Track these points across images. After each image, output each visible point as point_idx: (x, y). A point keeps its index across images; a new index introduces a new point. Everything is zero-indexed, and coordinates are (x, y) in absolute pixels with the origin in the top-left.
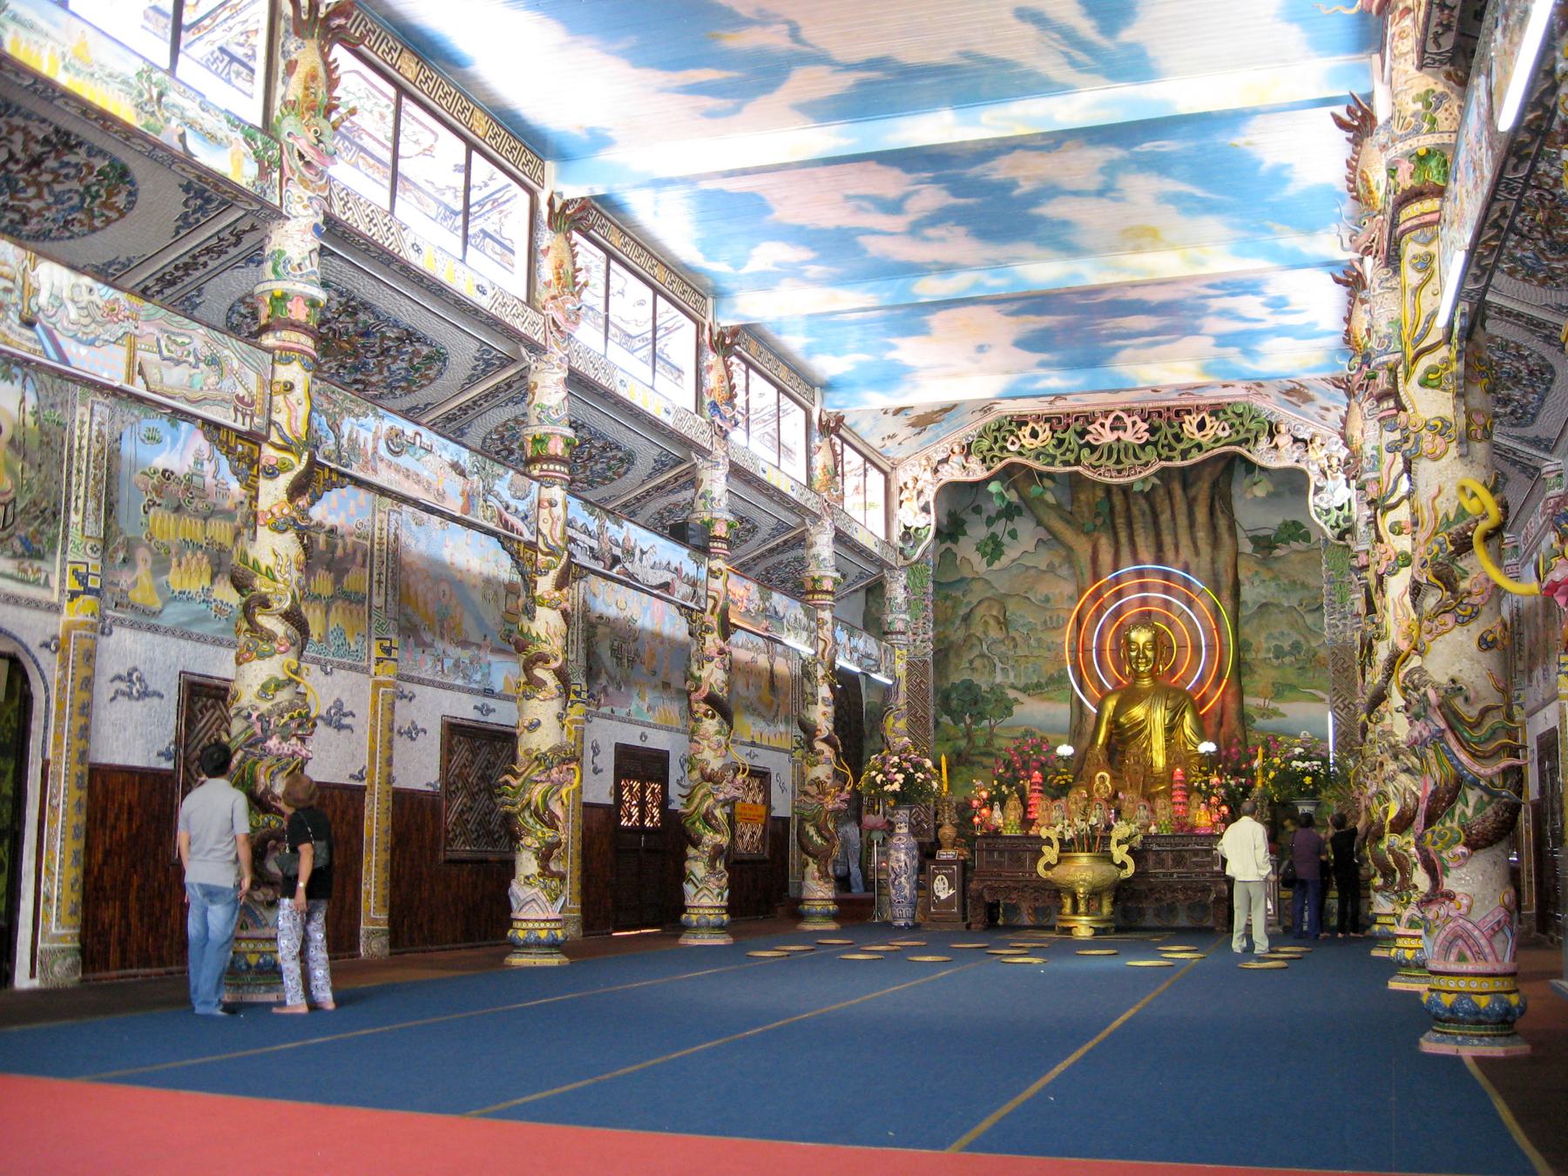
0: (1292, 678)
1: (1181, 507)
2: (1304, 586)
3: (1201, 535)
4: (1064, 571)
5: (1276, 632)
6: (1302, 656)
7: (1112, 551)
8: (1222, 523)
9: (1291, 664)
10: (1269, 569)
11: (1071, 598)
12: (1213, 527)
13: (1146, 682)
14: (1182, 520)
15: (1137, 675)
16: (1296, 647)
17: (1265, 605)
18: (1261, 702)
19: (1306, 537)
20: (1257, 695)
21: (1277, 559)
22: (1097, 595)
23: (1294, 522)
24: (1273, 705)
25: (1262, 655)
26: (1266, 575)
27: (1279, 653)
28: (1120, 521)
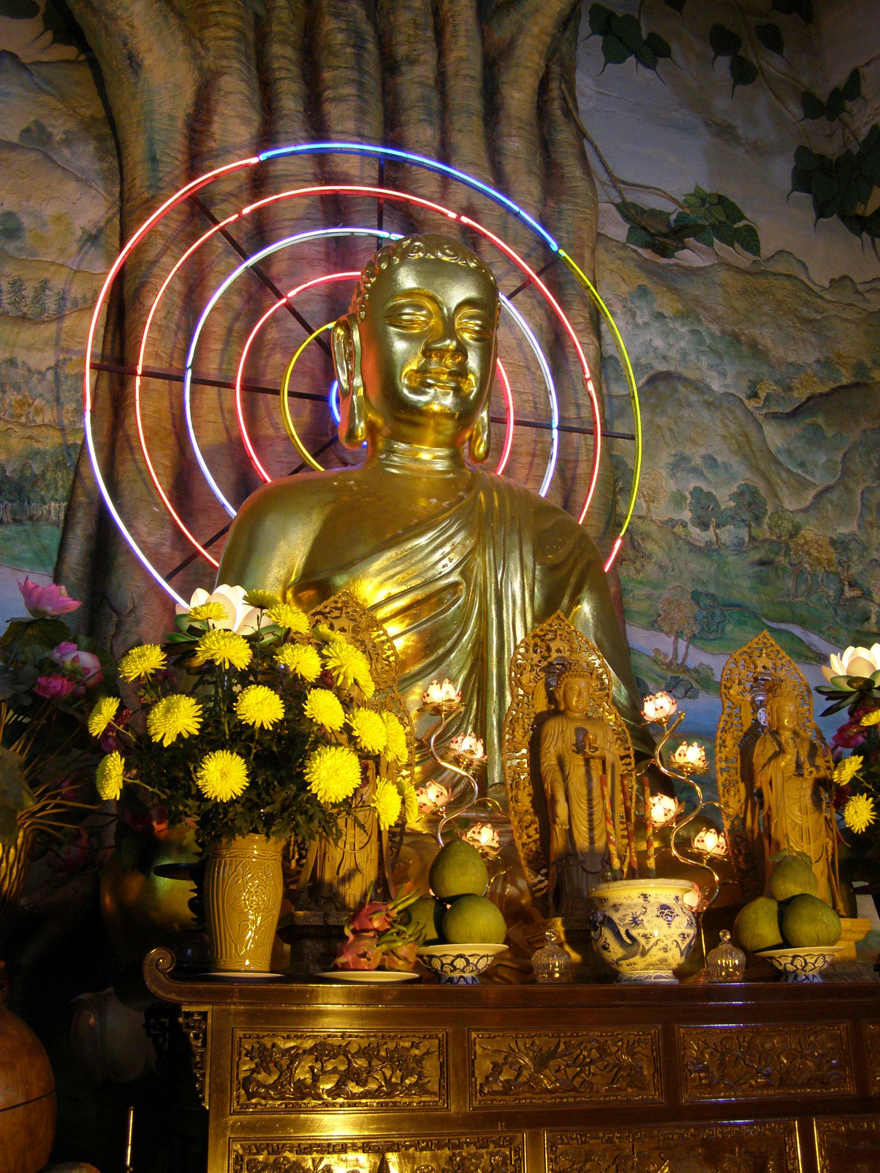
0: (743, 589)
1: (465, 52)
2: (757, 351)
3: (516, 145)
4: (85, 157)
5: (696, 455)
6: (764, 531)
7: (256, 118)
8: (564, 135)
9: (739, 548)
10: (671, 289)
11: (92, 238)
12: (545, 145)
13: (431, 457)
14: (466, 91)
15: (403, 417)
16: (751, 504)
17: (667, 376)
18: (664, 644)
19: (749, 240)
20: (653, 625)
21: (690, 272)
22: (200, 210)
23: (722, 200)
24: (697, 658)
25: (662, 511)
26: (667, 304)
27: (705, 511)
28: (283, 55)
